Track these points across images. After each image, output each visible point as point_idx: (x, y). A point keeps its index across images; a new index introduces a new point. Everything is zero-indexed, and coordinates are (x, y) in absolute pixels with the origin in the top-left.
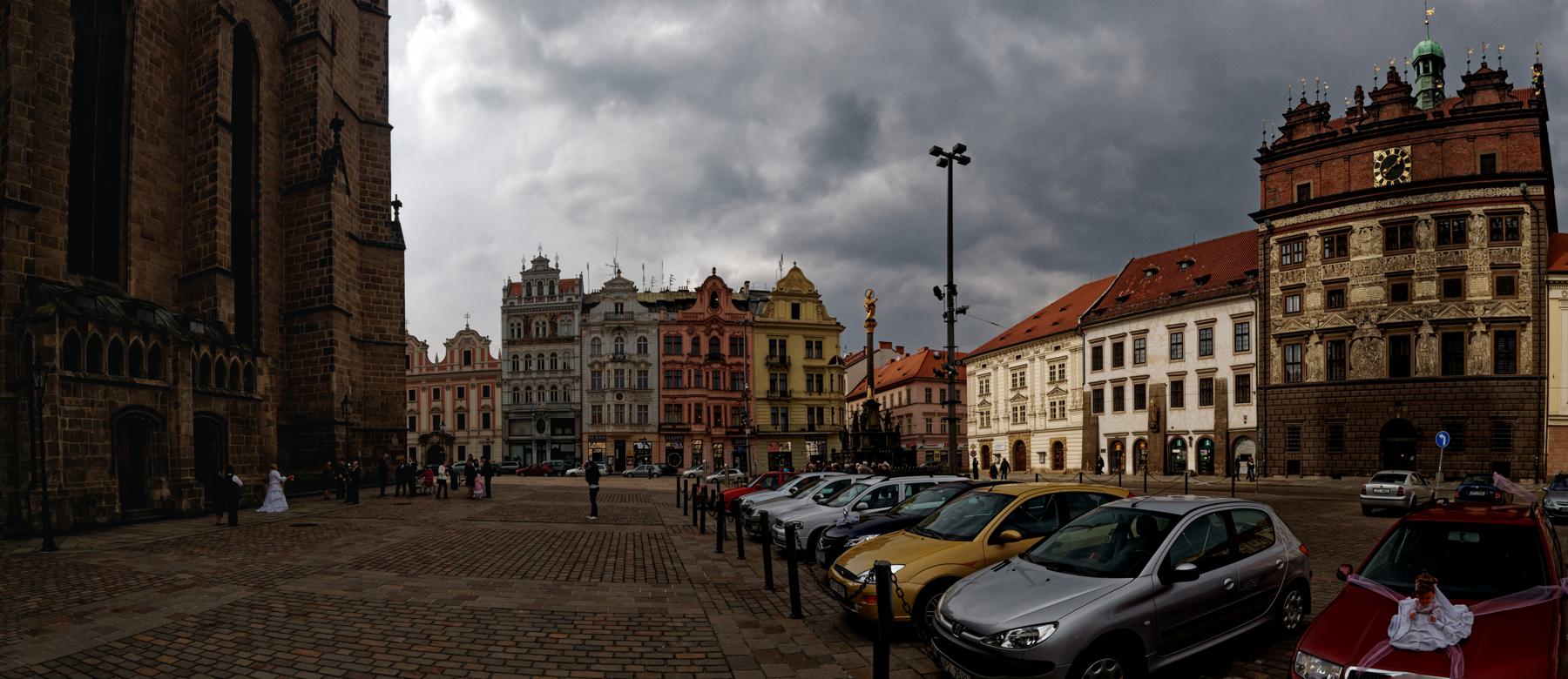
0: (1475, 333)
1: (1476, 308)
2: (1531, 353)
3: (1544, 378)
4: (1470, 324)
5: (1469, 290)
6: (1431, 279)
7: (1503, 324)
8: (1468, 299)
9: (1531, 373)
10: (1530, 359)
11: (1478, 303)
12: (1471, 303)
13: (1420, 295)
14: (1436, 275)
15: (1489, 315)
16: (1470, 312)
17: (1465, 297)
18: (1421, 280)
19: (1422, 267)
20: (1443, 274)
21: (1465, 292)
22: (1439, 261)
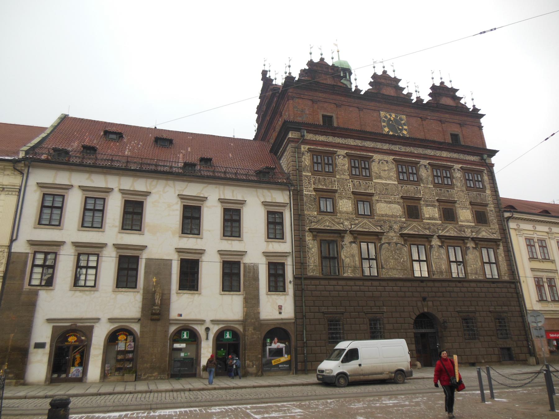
0: (468, 248)
1: (466, 230)
2: (505, 264)
3: (517, 282)
4: (466, 241)
5: (459, 217)
6: (433, 206)
7: (486, 243)
8: (460, 223)
9: (508, 279)
10: (506, 269)
11: (468, 227)
12: (462, 226)
13: (427, 216)
14: (437, 204)
15: (475, 236)
16: (463, 233)
17: (458, 222)
18: (427, 206)
19: (427, 197)
20: (442, 203)
21: (457, 218)
22: (437, 194)
